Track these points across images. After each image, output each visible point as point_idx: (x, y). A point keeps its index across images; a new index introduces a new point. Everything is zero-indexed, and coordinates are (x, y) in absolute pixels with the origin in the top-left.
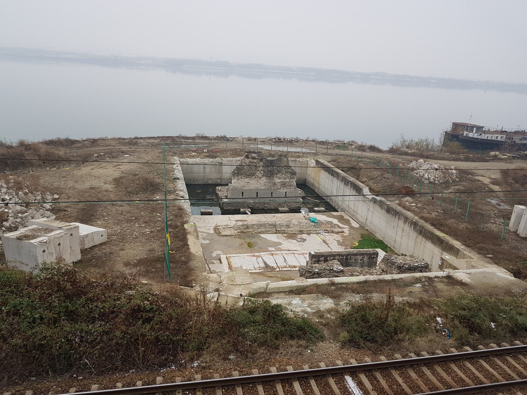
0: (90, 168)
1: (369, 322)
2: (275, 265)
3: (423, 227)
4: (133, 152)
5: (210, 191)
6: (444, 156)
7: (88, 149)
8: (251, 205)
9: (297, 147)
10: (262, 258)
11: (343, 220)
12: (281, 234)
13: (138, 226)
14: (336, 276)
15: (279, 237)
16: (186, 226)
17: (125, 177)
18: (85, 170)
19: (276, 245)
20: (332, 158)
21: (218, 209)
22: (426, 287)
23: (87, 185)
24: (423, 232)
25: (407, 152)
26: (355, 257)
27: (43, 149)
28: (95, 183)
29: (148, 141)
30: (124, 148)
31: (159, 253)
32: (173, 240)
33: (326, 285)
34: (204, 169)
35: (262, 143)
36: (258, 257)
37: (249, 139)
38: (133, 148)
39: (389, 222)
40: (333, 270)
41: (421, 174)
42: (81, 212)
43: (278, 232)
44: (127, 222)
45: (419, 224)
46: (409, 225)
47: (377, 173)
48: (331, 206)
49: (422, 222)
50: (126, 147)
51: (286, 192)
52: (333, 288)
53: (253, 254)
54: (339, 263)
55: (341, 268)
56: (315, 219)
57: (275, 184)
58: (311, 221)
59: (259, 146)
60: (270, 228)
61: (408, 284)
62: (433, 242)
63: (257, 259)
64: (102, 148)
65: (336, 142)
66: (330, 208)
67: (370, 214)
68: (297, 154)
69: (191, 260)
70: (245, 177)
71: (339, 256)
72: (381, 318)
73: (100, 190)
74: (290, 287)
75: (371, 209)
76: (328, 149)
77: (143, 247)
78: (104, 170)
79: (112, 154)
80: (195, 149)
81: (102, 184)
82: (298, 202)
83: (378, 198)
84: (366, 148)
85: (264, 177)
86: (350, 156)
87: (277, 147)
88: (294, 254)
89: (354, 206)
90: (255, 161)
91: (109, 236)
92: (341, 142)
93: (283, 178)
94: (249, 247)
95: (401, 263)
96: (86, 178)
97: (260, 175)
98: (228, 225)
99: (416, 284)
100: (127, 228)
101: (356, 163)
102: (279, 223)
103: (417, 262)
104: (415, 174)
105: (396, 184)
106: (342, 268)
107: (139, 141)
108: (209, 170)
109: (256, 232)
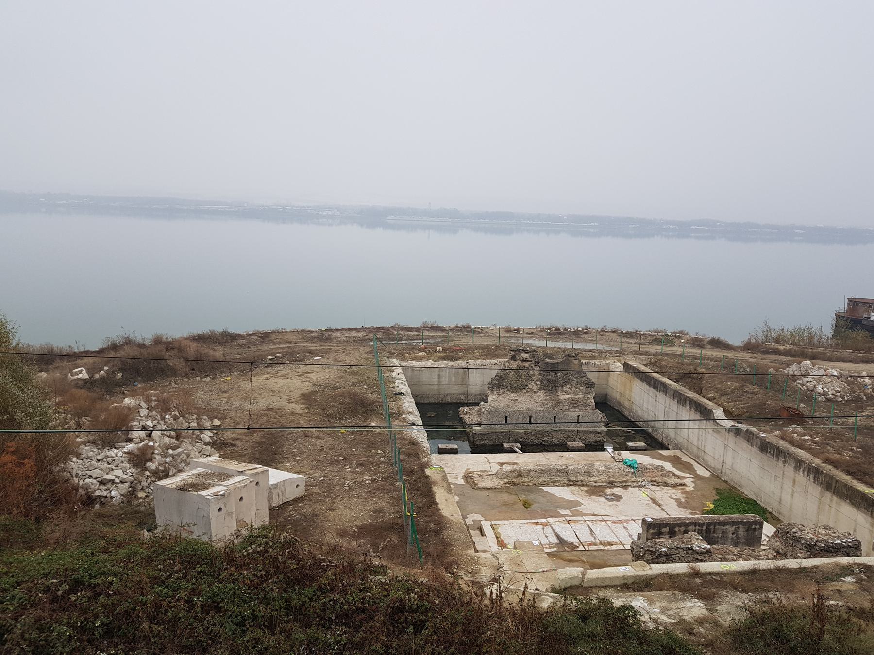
0: (263, 377)
1: (788, 641)
2: (575, 541)
3: (832, 477)
4: (326, 352)
5: (449, 414)
6: (843, 356)
7: (256, 349)
8: (521, 438)
9: (587, 341)
10: (552, 528)
11: (681, 463)
12: (577, 488)
13: (350, 472)
14: (697, 559)
15: (575, 493)
16: (428, 471)
17: (318, 392)
18: (258, 380)
19: (571, 505)
20: (649, 360)
21: (466, 445)
22: (865, 583)
23: (261, 404)
24: (834, 485)
25: (777, 349)
26: (722, 528)
27: (193, 348)
28: (274, 401)
29: (347, 334)
30: (312, 346)
31: (390, 515)
32: (411, 493)
33: (685, 574)
34: (439, 379)
35: (529, 336)
36: (544, 525)
37: (508, 330)
38: (326, 346)
39: (766, 468)
40: (692, 549)
41: (811, 386)
42: (258, 447)
43: (572, 483)
44: (332, 464)
45: (825, 472)
46: (806, 473)
47: (732, 385)
48: (655, 440)
49: (827, 468)
50: (315, 345)
51: (578, 416)
52: (698, 580)
53: (536, 520)
54: (701, 538)
55: (706, 546)
56: (634, 462)
57: (560, 402)
58: (628, 466)
59: (526, 341)
60: (559, 477)
61: (830, 576)
62: (853, 504)
63: (543, 529)
64: (279, 347)
65: (653, 334)
66: (655, 444)
67: (730, 454)
68: (590, 353)
69: (446, 528)
70: (510, 390)
71: (695, 526)
72: (810, 635)
73: (283, 413)
74: (624, 578)
75: (731, 445)
76: (640, 344)
77: (365, 505)
78: (286, 381)
79: (295, 355)
80: (423, 346)
81: (286, 403)
82: (600, 433)
83: (743, 426)
84: (705, 342)
85: (542, 391)
86: (680, 356)
87: (553, 343)
88: (605, 521)
89: (698, 439)
90: (527, 365)
91: (308, 486)
92: (661, 334)
93: (572, 392)
94: (527, 508)
95: (811, 538)
96: (259, 394)
98: (485, 471)
99: (844, 578)
100: (333, 474)
101: (692, 367)
102: (572, 467)
103: (839, 538)
104: (799, 386)
105: (769, 402)
106: (709, 547)
107: (333, 334)
108: (447, 380)
109: (534, 482)
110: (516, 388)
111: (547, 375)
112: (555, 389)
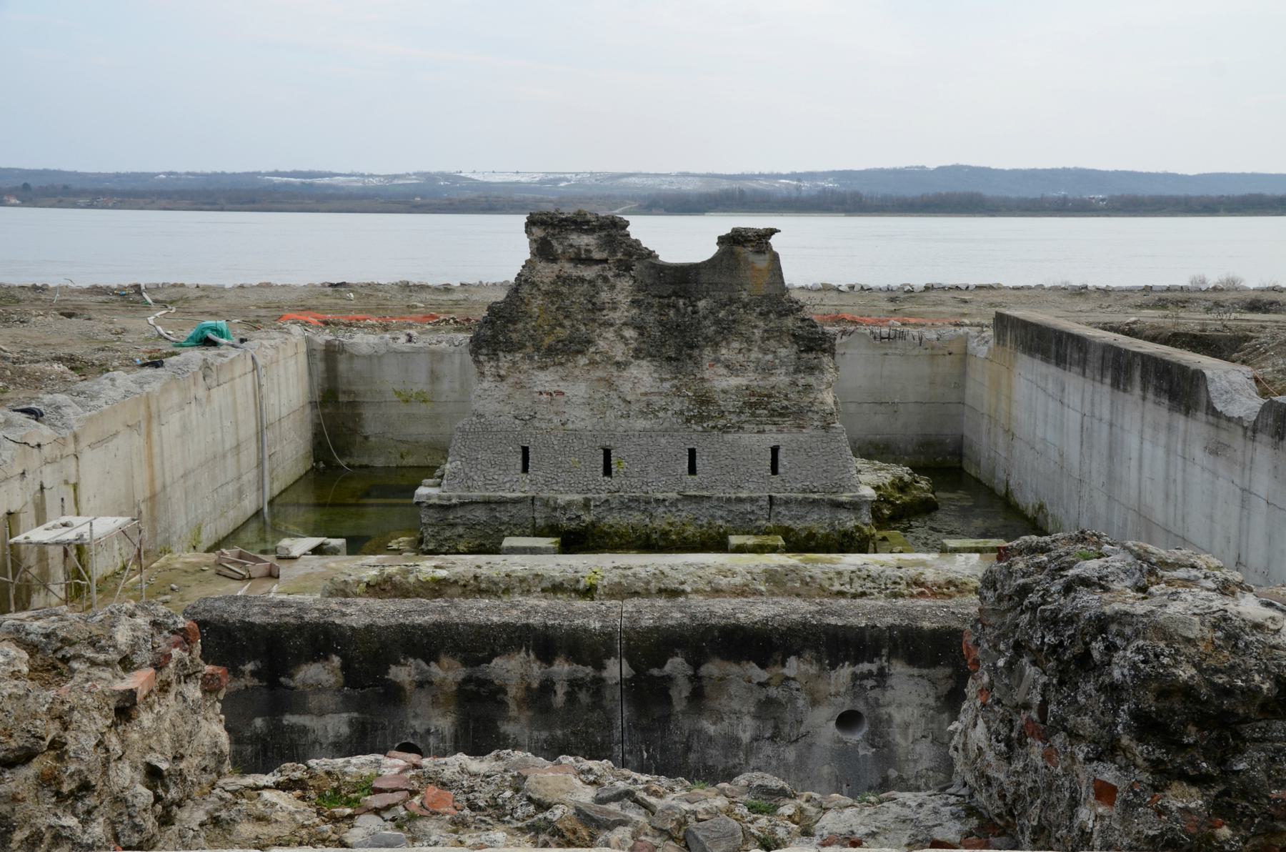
70: (531, 358)
85: (644, 363)
90: (589, 273)
97: (619, 352)
110: (551, 351)
111: (661, 306)
112: (690, 357)
